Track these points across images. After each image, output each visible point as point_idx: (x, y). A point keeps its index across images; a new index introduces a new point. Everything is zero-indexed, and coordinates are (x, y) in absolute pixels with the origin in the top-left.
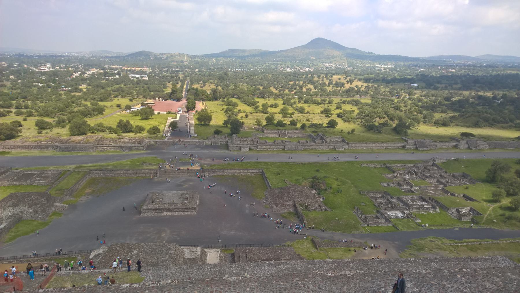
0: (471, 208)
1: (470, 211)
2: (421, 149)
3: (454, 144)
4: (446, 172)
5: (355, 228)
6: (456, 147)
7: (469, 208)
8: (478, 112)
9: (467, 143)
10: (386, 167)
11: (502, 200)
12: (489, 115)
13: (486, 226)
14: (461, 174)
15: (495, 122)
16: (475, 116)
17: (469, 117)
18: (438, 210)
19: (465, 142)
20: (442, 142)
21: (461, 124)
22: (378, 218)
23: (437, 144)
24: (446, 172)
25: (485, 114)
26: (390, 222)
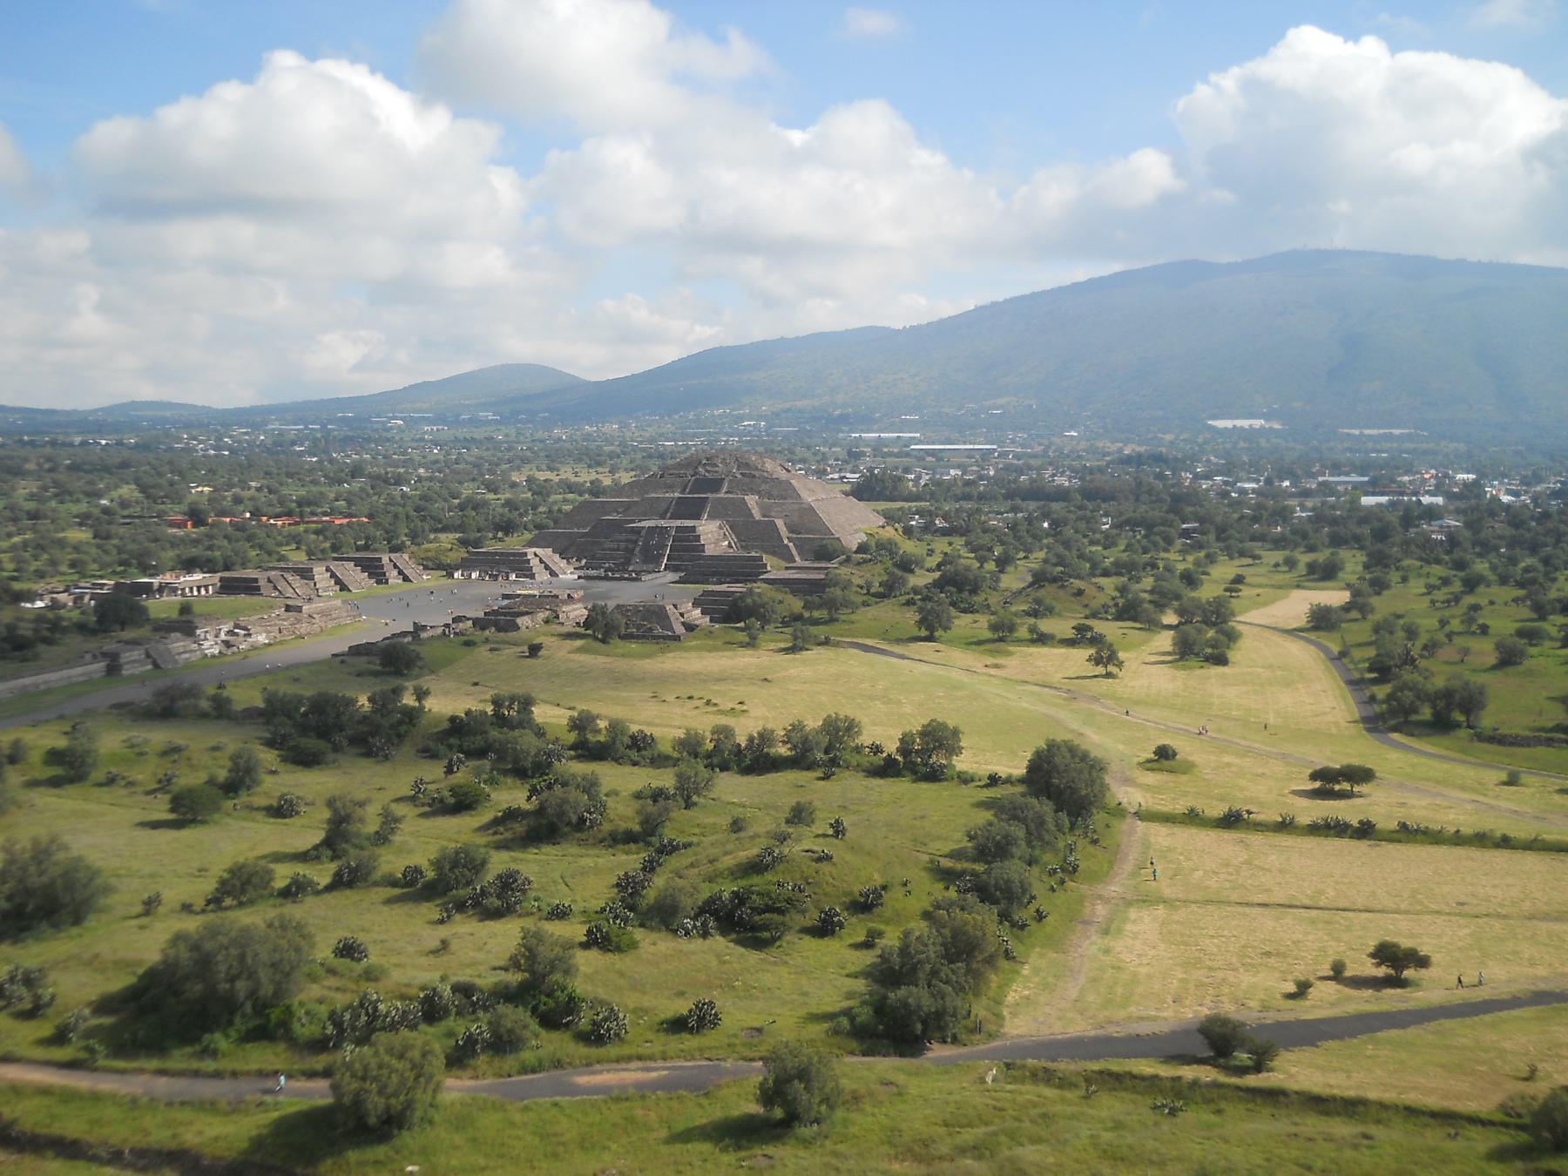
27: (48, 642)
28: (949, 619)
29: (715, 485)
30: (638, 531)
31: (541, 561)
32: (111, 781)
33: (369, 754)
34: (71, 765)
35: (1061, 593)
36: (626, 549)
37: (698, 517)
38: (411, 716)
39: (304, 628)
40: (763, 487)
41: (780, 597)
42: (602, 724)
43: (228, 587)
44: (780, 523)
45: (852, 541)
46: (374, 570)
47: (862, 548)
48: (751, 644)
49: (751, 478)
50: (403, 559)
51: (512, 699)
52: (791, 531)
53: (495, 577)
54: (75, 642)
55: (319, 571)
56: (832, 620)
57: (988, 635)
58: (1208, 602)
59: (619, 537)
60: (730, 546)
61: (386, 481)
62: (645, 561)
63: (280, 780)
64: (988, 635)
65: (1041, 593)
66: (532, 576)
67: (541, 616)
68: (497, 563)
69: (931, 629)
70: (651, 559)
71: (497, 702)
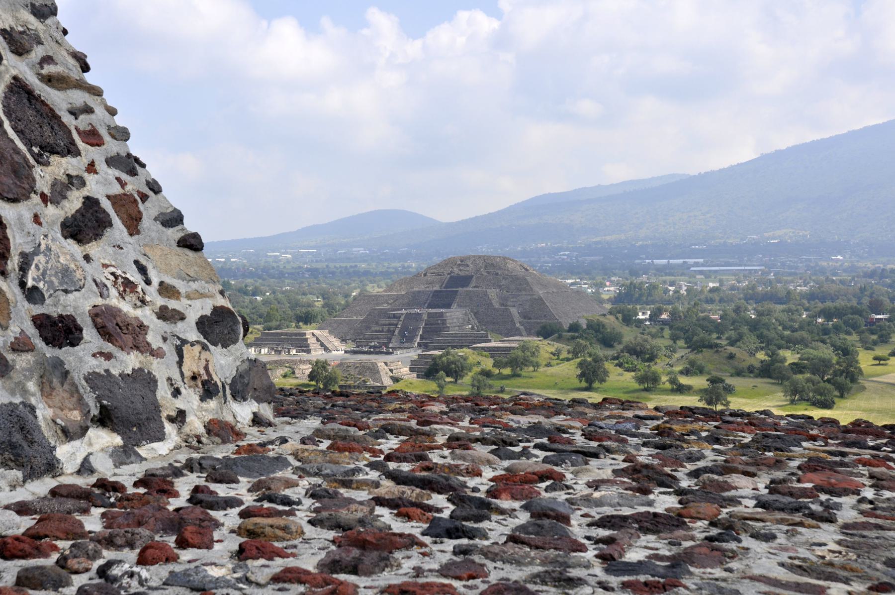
28: (606, 373)
31: (318, 340)
35: (716, 357)
36: (389, 331)
37: (448, 306)
40: (503, 282)
41: (479, 358)
44: (514, 311)
45: (566, 323)
47: (574, 328)
52: (525, 317)
53: (280, 352)
56: (515, 375)
57: (637, 386)
59: (383, 322)
60: (473, 328)
61: (246, 293)
64: (637, 386)
65: (700, 356)
66: (308, 351)
68: (282, 341)
69: (590, 382)
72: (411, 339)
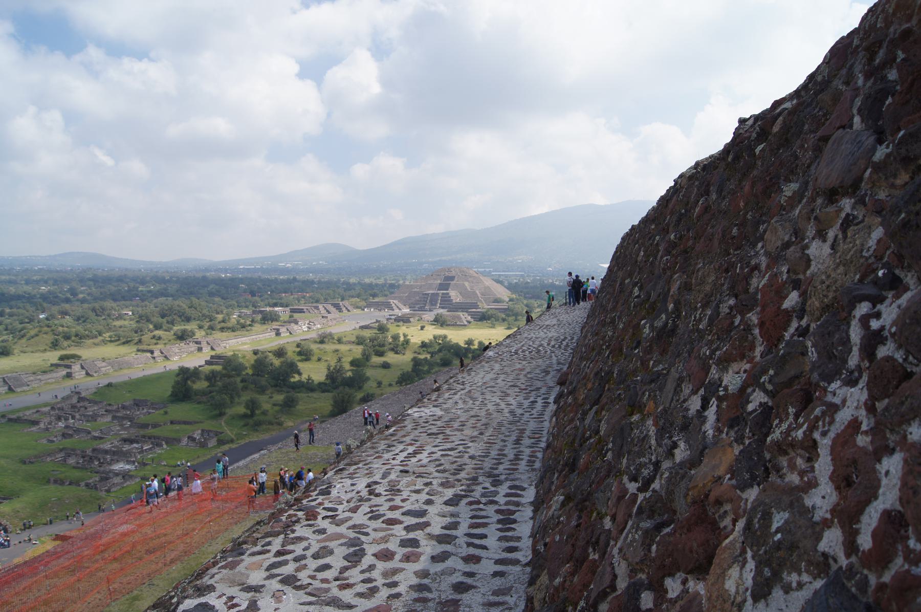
0: (203, 431)
1: (202, 435)
2: (19, 390)
3: (64, 373)
4: (110, 405)
5: (98, 499)
6: (69, 376)
7: (200, 432)
8: (48, 326)
9: (83, 368)
10: (10, 420)
11: (227, 411)
12: (65, 329)
13: (242, 442)
14: (132, 402)
15: (81, 338)
16: (46, 333)
17: (37, 335)
18: (165, 446)
19: (79, 366)
20: (45, 372)
21: (29, 349)
22: (107, 479)
23: (39, 377)
24: (110, 405)
25: (61, 329)
26: (131, 477)
27: (250, 325)
29: (452, 278)
30: (428, 294)
32: (319, 360)
33: (397, 353)
34: (306, 355)
38: (407, 342)
39: (330, 323)
42: (476, 343)
43: (293, 311)
46: (337, 307)
48: (493, 327)
49: (466, 276)
50: (346, 303)
51: (440, 336)
54: (257, 327)
55: (321, 307)
58: (826, 233)
62: (432, 305)
63: (376, 360)
67: (417, 318)
70: (433, 303)
71: (435, 337)
72: (436, 305)
